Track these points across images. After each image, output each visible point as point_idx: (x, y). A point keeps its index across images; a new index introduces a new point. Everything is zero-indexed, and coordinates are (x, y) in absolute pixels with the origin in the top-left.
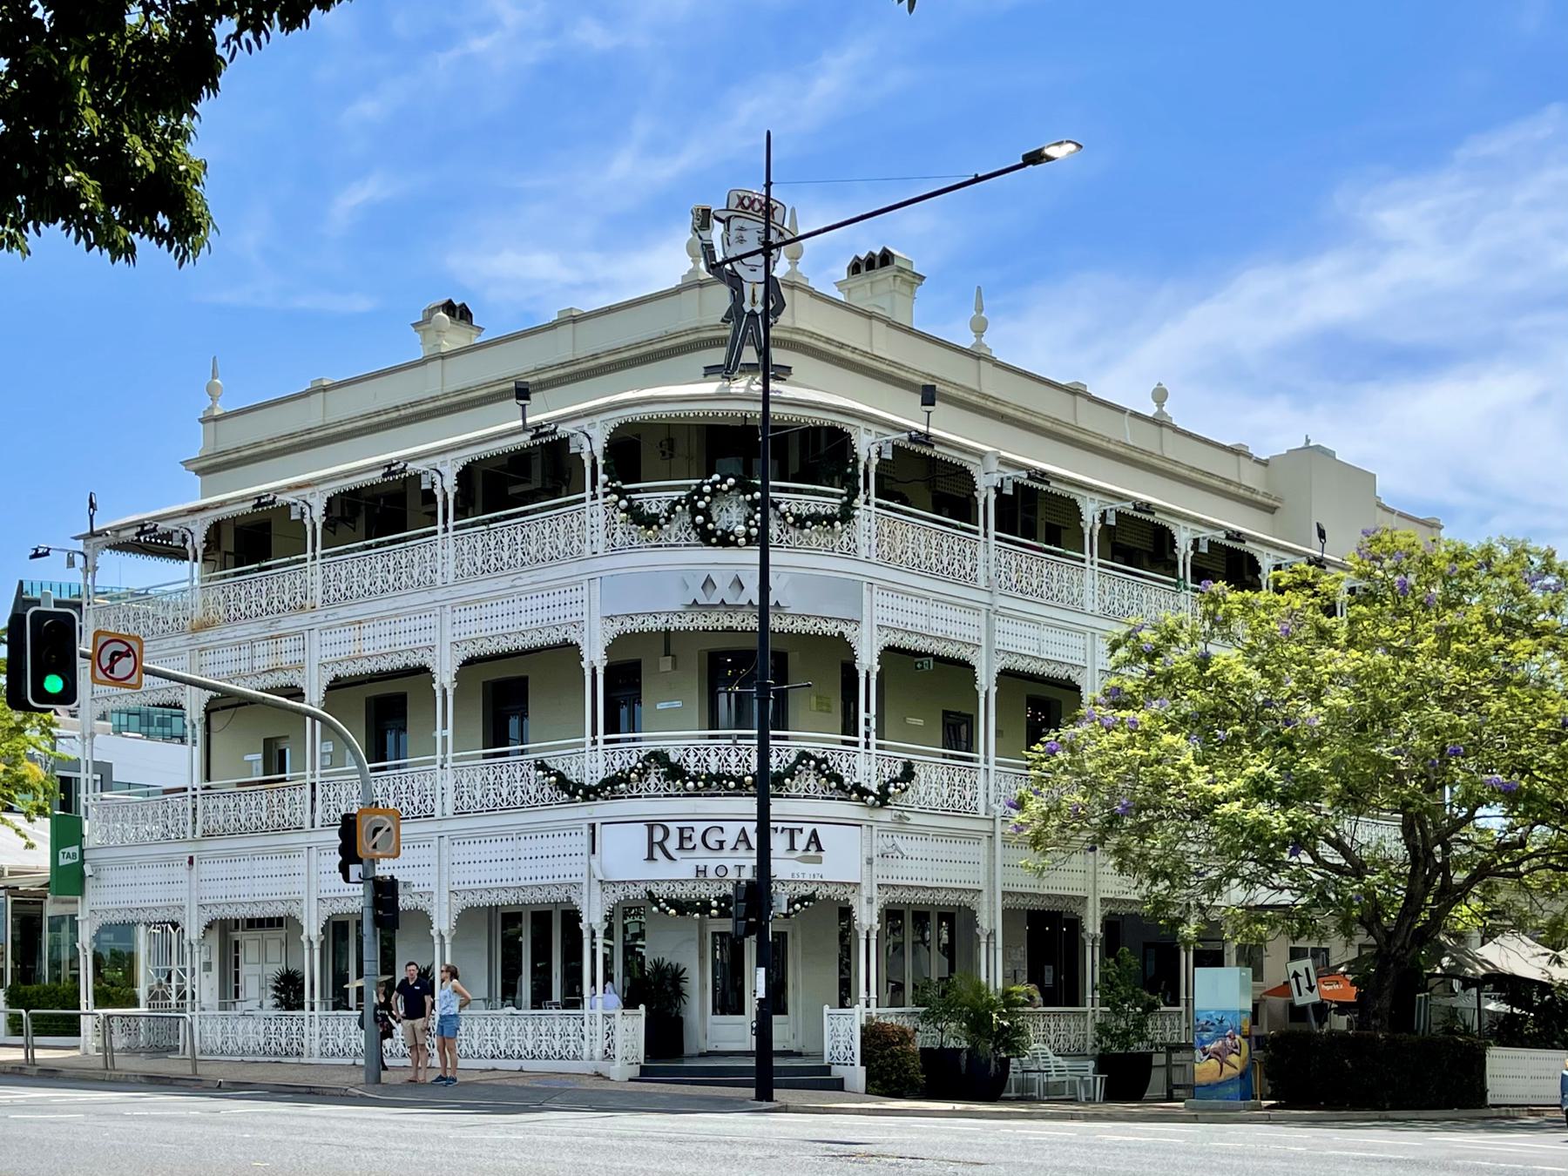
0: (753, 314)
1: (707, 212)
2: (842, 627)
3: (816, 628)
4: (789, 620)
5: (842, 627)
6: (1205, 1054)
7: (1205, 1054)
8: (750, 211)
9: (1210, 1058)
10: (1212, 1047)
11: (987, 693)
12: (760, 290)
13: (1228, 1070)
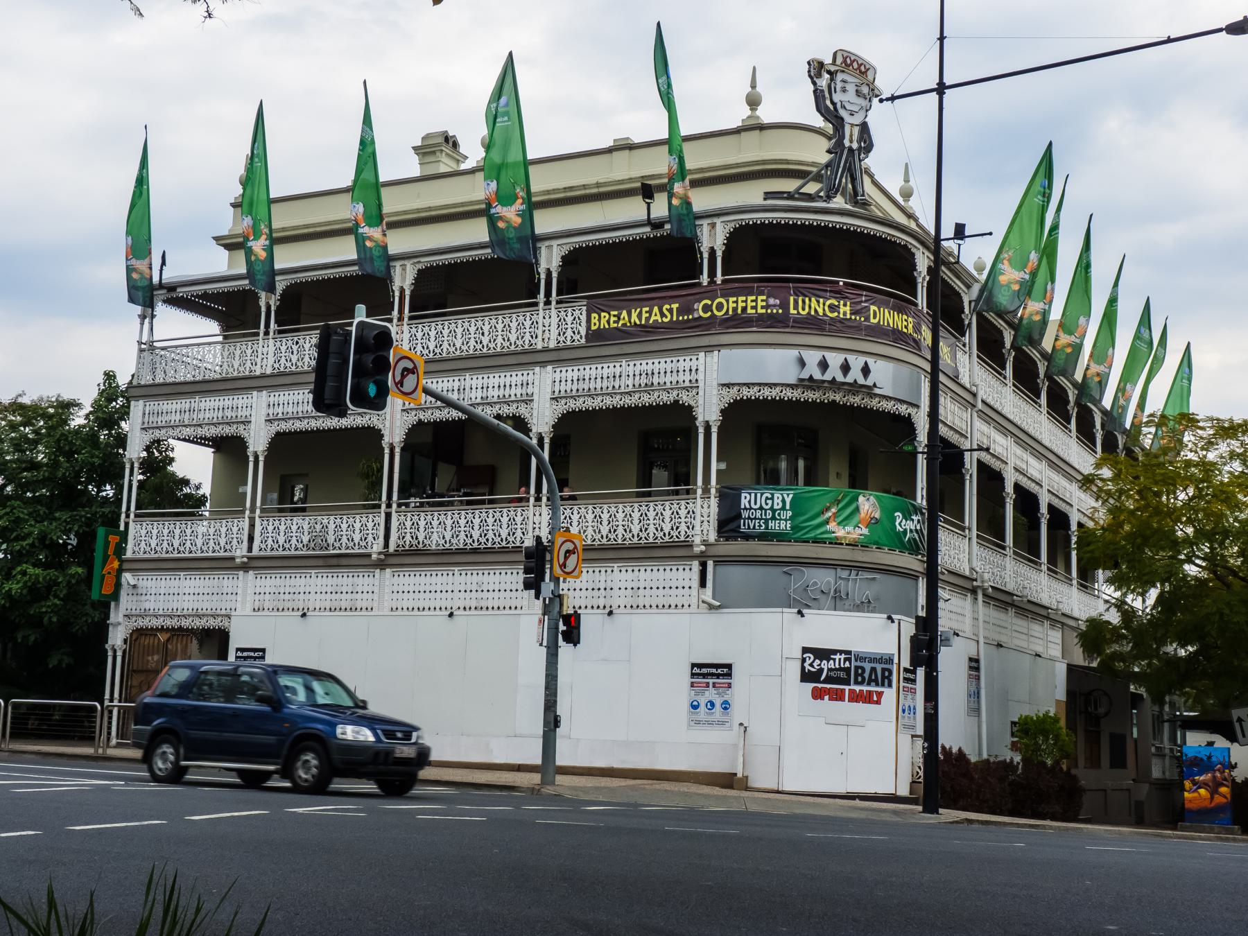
0: (851, 150)
1: (821, 64)
2: (910, 410)
4: (877, 399)
6: (1194, 785)
7: (1194, 785)
9: (1200, 788)
10: (1202, 778)
11: (971, 475)
12: (856, 130)
13: (1218, 799)
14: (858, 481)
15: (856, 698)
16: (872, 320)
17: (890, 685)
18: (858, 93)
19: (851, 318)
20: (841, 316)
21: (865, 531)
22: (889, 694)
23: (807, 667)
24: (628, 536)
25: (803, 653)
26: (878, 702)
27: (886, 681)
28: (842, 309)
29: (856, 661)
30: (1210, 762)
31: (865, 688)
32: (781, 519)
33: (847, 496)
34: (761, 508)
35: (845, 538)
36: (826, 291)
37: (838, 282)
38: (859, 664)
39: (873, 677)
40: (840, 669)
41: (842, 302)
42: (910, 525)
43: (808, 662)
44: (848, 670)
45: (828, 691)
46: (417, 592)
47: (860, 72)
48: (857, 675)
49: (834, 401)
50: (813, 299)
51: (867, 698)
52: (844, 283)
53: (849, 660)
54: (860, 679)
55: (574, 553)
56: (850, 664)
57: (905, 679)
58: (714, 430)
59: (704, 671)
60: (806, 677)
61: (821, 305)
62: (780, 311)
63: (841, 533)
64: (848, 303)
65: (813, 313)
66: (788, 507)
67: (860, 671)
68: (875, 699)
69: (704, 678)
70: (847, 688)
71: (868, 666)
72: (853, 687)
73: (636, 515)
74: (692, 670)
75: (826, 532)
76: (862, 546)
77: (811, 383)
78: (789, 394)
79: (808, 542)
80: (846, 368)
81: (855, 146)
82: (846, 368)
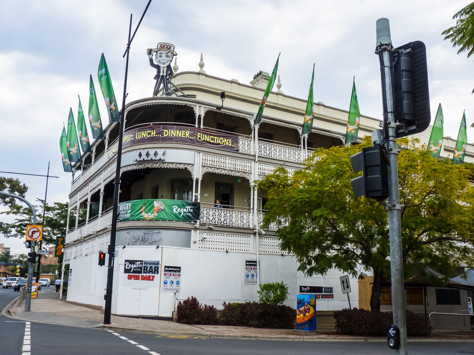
2: (187, 166)
3: (176, 167)
4: (166, 164)
5: (187, 166)
8: (164, 48)
9: (301, 313)
14: (155, 196)
15: (144, 278)
16: (165, 135)
17: (158, 273)
18: (167, 56)
19: (155, 136)
20: (152, 136)
21: (156, 214)
22: (157, 276)
23: (127, 267)
24: (220, 222)
25: (125, 262)
26: (152, 280)
27: (156, 271)
28: (152, 133)
29: (144, 264)
30: (304, 301)
31: (147, 275)
32: (128, 213)
33: (149, 202)
34: (124, 210)
35: (148, 217)
36: (147, 128)
37: (150, 124)
38: (145, 265)
39: (151, 270)
40: (138, 268)
41: (152, 131)
42: (182, 210)
43: (127, 265)
44: (141, 268)
45: (133, 276)
46: (267, 245)
47: (168, 48)
48: (144, 269)
49: (148, 167)
50: (143, 132)
51: (148, 279)
52: (153, 124)
53: (142, 264)
54: (145, 271)
55: (38, 232)
56: (142, 266)
57: (165, 270)
58: (200, 182)
59: (170, 269)
60: (127, 271)
61: (145, 134)
62: (133, 139)
63: (146, 216)
64: (155, 131)
65: (142, 137)
66: (130, 209)
67: (146, 268)
68: (151, 278)
69: (170, 272)
70: (140, 275)
71: (149, 266)
72: (143, 274)
73: (223, 214)
74: (165, 268)
75: (141, 216)
76: (155, 220)
77: (140, 162)
78: (134, 168)
79: (135, 220)
80: (148, 155)
81: (165, 74)
82: (148, 155)
